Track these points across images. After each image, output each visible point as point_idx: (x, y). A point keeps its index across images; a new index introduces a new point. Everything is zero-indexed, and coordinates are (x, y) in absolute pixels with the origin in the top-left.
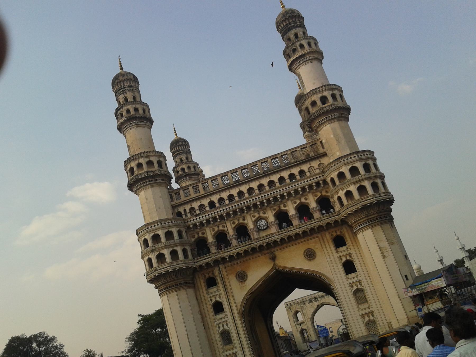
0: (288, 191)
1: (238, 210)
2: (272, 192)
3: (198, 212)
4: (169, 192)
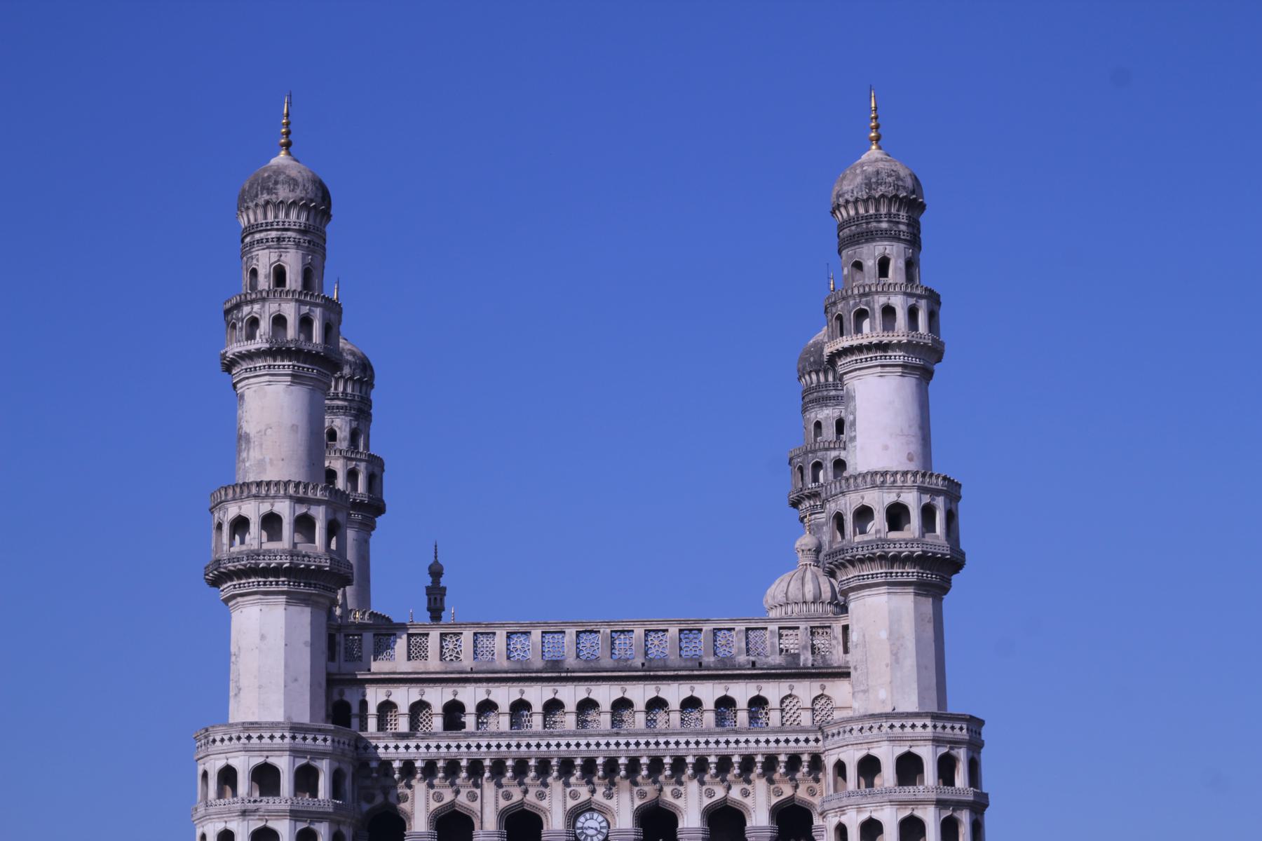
0: (701, 752)
1: (532, 762)
2: (652, 741)
3: (403, 725)
4: (329, 627)
